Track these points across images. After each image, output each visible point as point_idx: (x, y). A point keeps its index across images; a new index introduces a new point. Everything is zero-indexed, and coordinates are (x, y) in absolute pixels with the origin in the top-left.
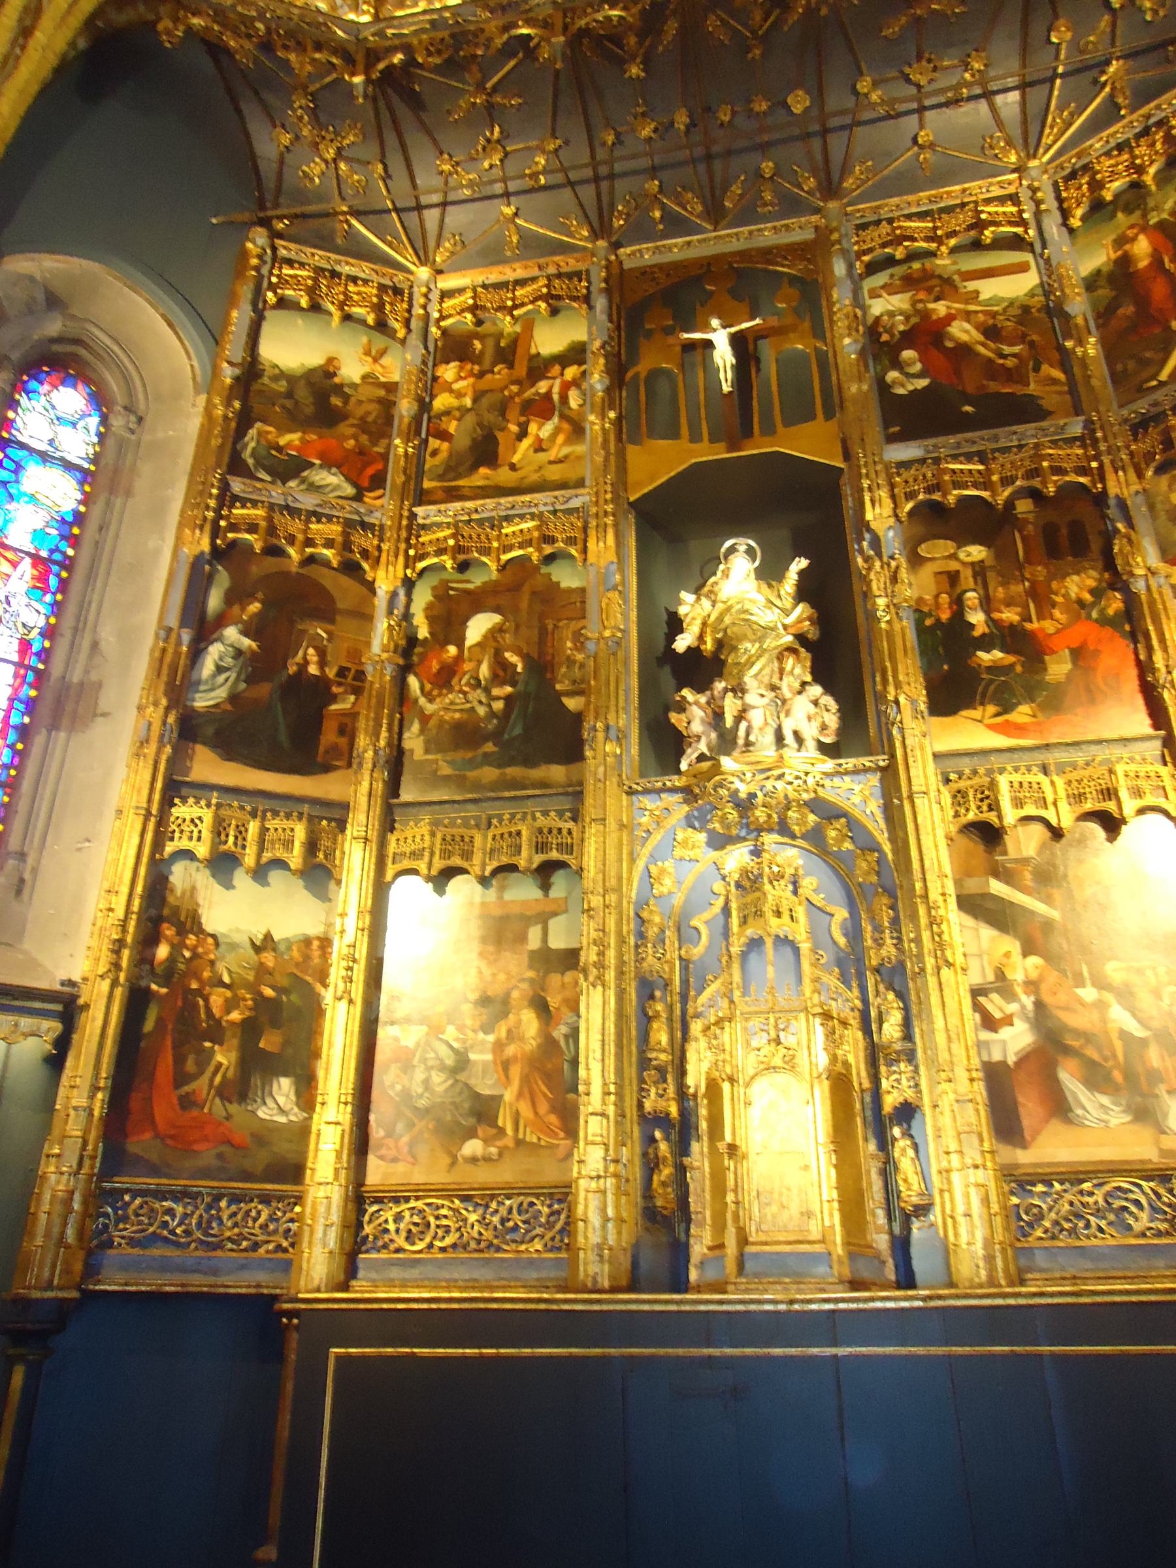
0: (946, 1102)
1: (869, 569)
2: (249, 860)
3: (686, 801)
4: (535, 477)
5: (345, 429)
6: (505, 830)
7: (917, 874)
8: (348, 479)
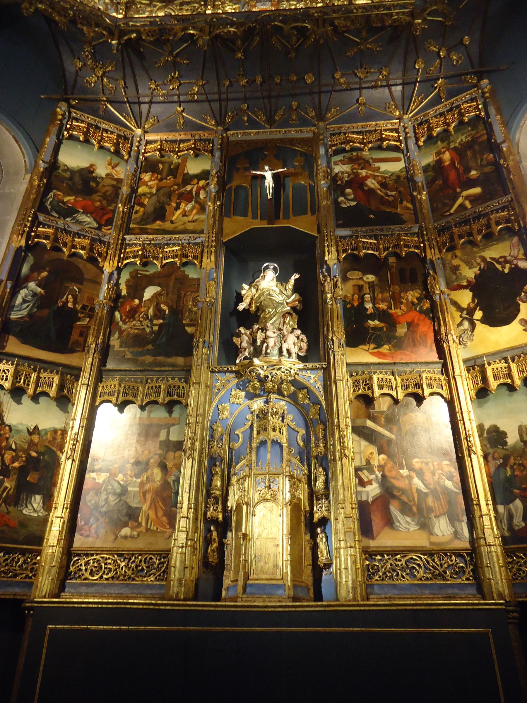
0: (341, 517)
1: (325, 281)
2: (30, 391)
3: (237, 377)
4: (181, 227)
5: (96, 197)
6: (154, 385)
7: (335, 416)
8: (95, 220)
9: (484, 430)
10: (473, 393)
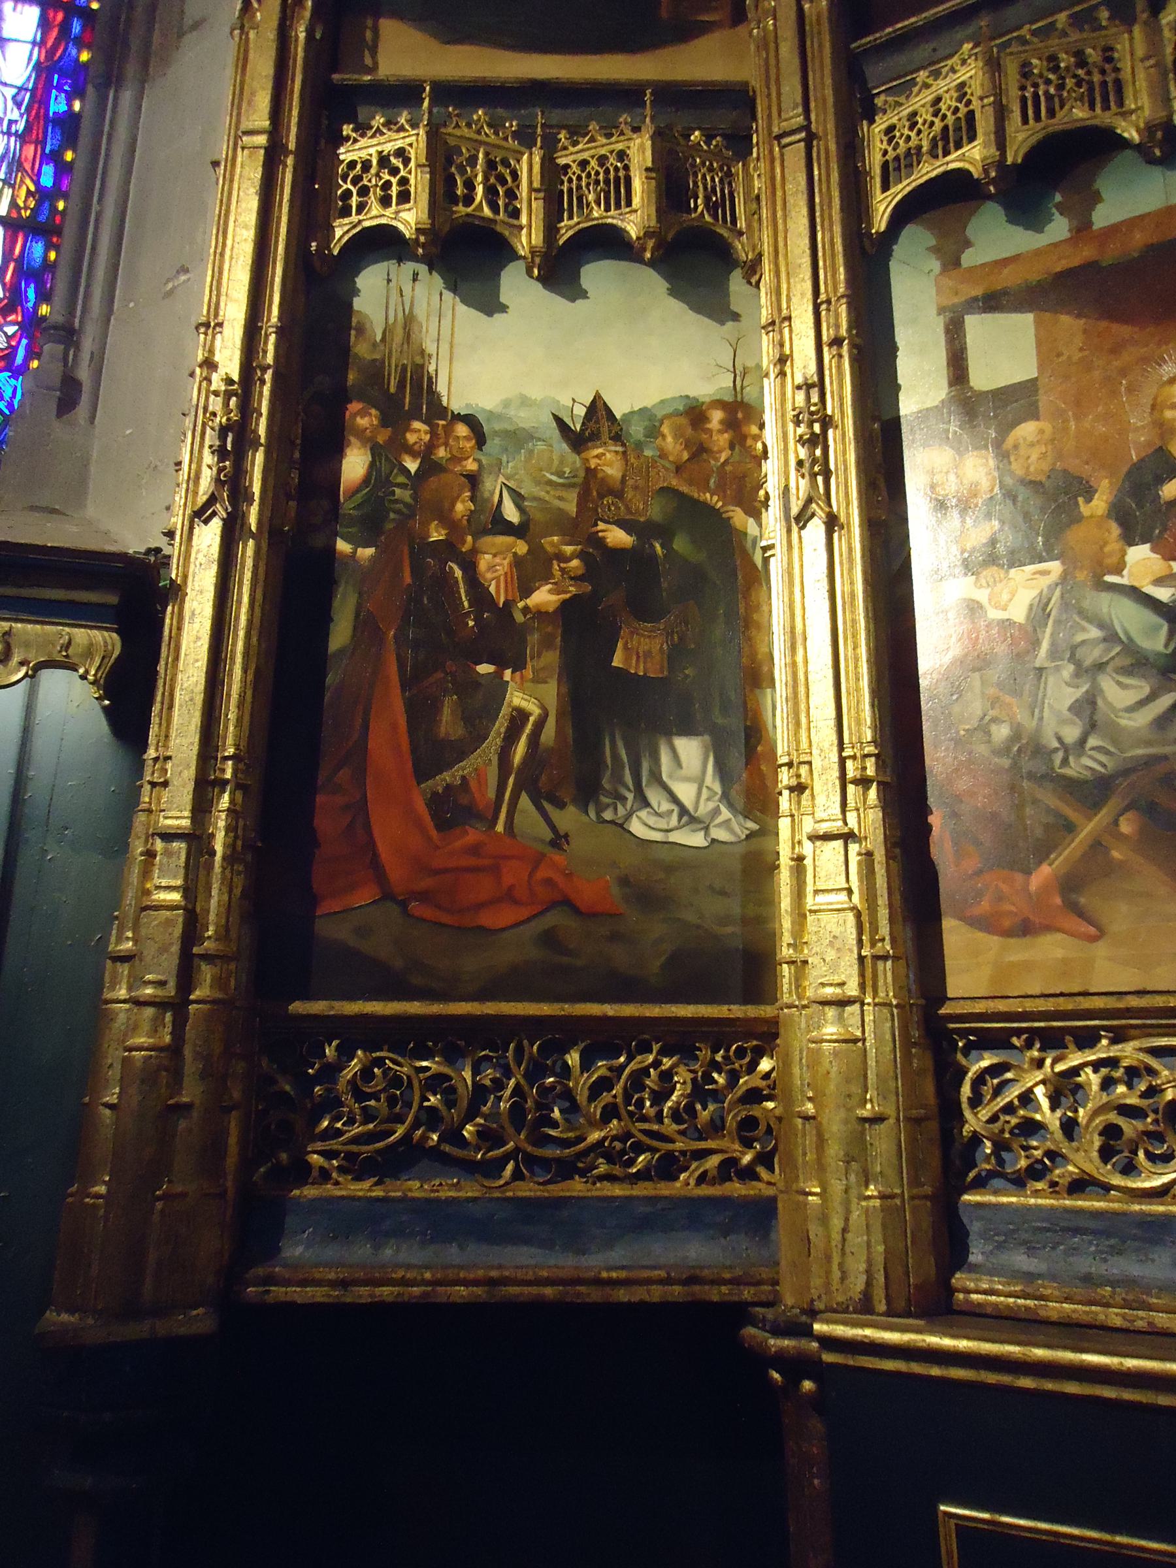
2: (528, 237)
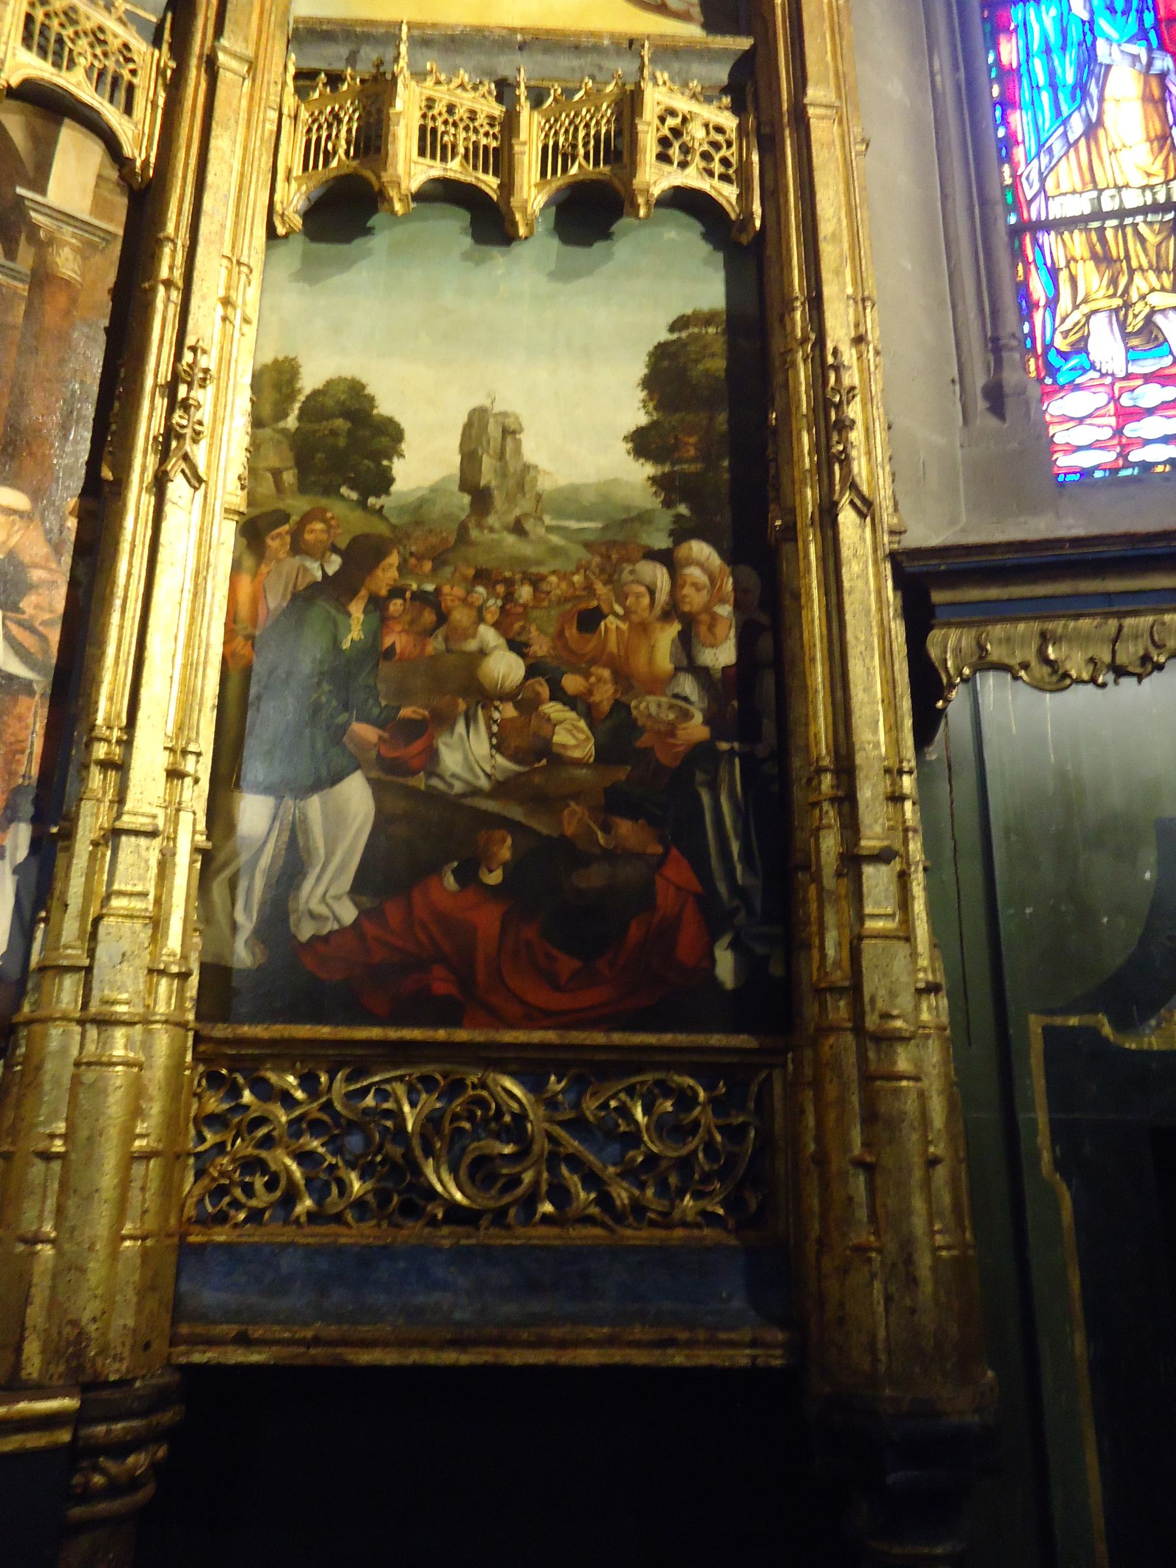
9: (291, 396)
10: (293, 198)
